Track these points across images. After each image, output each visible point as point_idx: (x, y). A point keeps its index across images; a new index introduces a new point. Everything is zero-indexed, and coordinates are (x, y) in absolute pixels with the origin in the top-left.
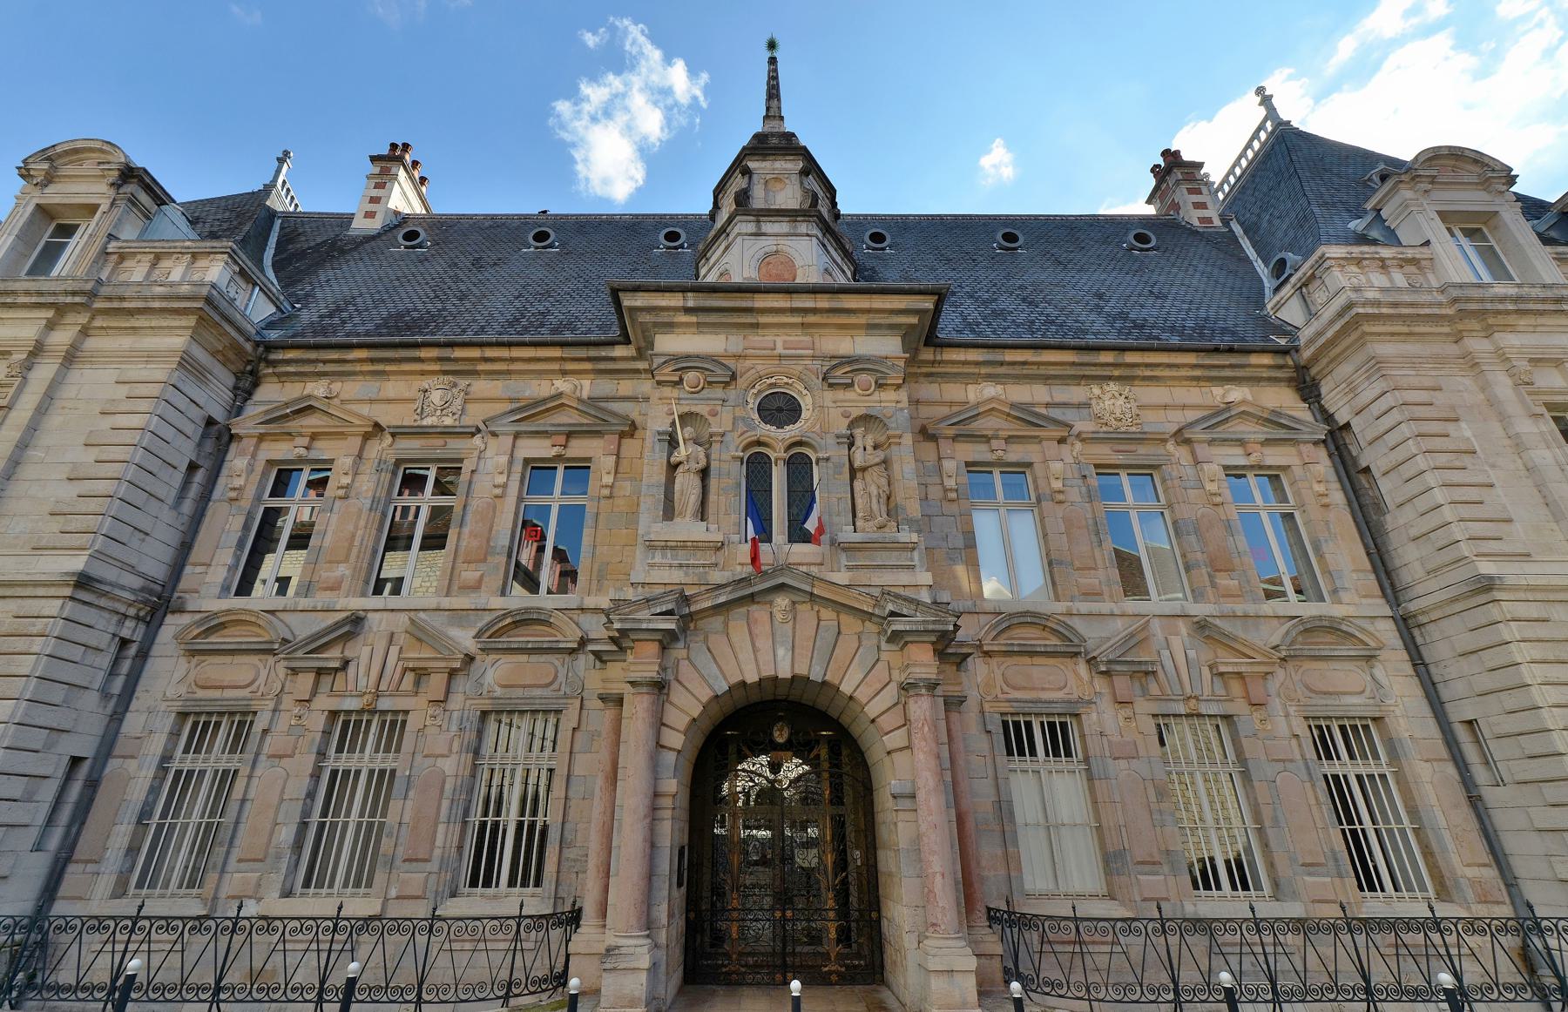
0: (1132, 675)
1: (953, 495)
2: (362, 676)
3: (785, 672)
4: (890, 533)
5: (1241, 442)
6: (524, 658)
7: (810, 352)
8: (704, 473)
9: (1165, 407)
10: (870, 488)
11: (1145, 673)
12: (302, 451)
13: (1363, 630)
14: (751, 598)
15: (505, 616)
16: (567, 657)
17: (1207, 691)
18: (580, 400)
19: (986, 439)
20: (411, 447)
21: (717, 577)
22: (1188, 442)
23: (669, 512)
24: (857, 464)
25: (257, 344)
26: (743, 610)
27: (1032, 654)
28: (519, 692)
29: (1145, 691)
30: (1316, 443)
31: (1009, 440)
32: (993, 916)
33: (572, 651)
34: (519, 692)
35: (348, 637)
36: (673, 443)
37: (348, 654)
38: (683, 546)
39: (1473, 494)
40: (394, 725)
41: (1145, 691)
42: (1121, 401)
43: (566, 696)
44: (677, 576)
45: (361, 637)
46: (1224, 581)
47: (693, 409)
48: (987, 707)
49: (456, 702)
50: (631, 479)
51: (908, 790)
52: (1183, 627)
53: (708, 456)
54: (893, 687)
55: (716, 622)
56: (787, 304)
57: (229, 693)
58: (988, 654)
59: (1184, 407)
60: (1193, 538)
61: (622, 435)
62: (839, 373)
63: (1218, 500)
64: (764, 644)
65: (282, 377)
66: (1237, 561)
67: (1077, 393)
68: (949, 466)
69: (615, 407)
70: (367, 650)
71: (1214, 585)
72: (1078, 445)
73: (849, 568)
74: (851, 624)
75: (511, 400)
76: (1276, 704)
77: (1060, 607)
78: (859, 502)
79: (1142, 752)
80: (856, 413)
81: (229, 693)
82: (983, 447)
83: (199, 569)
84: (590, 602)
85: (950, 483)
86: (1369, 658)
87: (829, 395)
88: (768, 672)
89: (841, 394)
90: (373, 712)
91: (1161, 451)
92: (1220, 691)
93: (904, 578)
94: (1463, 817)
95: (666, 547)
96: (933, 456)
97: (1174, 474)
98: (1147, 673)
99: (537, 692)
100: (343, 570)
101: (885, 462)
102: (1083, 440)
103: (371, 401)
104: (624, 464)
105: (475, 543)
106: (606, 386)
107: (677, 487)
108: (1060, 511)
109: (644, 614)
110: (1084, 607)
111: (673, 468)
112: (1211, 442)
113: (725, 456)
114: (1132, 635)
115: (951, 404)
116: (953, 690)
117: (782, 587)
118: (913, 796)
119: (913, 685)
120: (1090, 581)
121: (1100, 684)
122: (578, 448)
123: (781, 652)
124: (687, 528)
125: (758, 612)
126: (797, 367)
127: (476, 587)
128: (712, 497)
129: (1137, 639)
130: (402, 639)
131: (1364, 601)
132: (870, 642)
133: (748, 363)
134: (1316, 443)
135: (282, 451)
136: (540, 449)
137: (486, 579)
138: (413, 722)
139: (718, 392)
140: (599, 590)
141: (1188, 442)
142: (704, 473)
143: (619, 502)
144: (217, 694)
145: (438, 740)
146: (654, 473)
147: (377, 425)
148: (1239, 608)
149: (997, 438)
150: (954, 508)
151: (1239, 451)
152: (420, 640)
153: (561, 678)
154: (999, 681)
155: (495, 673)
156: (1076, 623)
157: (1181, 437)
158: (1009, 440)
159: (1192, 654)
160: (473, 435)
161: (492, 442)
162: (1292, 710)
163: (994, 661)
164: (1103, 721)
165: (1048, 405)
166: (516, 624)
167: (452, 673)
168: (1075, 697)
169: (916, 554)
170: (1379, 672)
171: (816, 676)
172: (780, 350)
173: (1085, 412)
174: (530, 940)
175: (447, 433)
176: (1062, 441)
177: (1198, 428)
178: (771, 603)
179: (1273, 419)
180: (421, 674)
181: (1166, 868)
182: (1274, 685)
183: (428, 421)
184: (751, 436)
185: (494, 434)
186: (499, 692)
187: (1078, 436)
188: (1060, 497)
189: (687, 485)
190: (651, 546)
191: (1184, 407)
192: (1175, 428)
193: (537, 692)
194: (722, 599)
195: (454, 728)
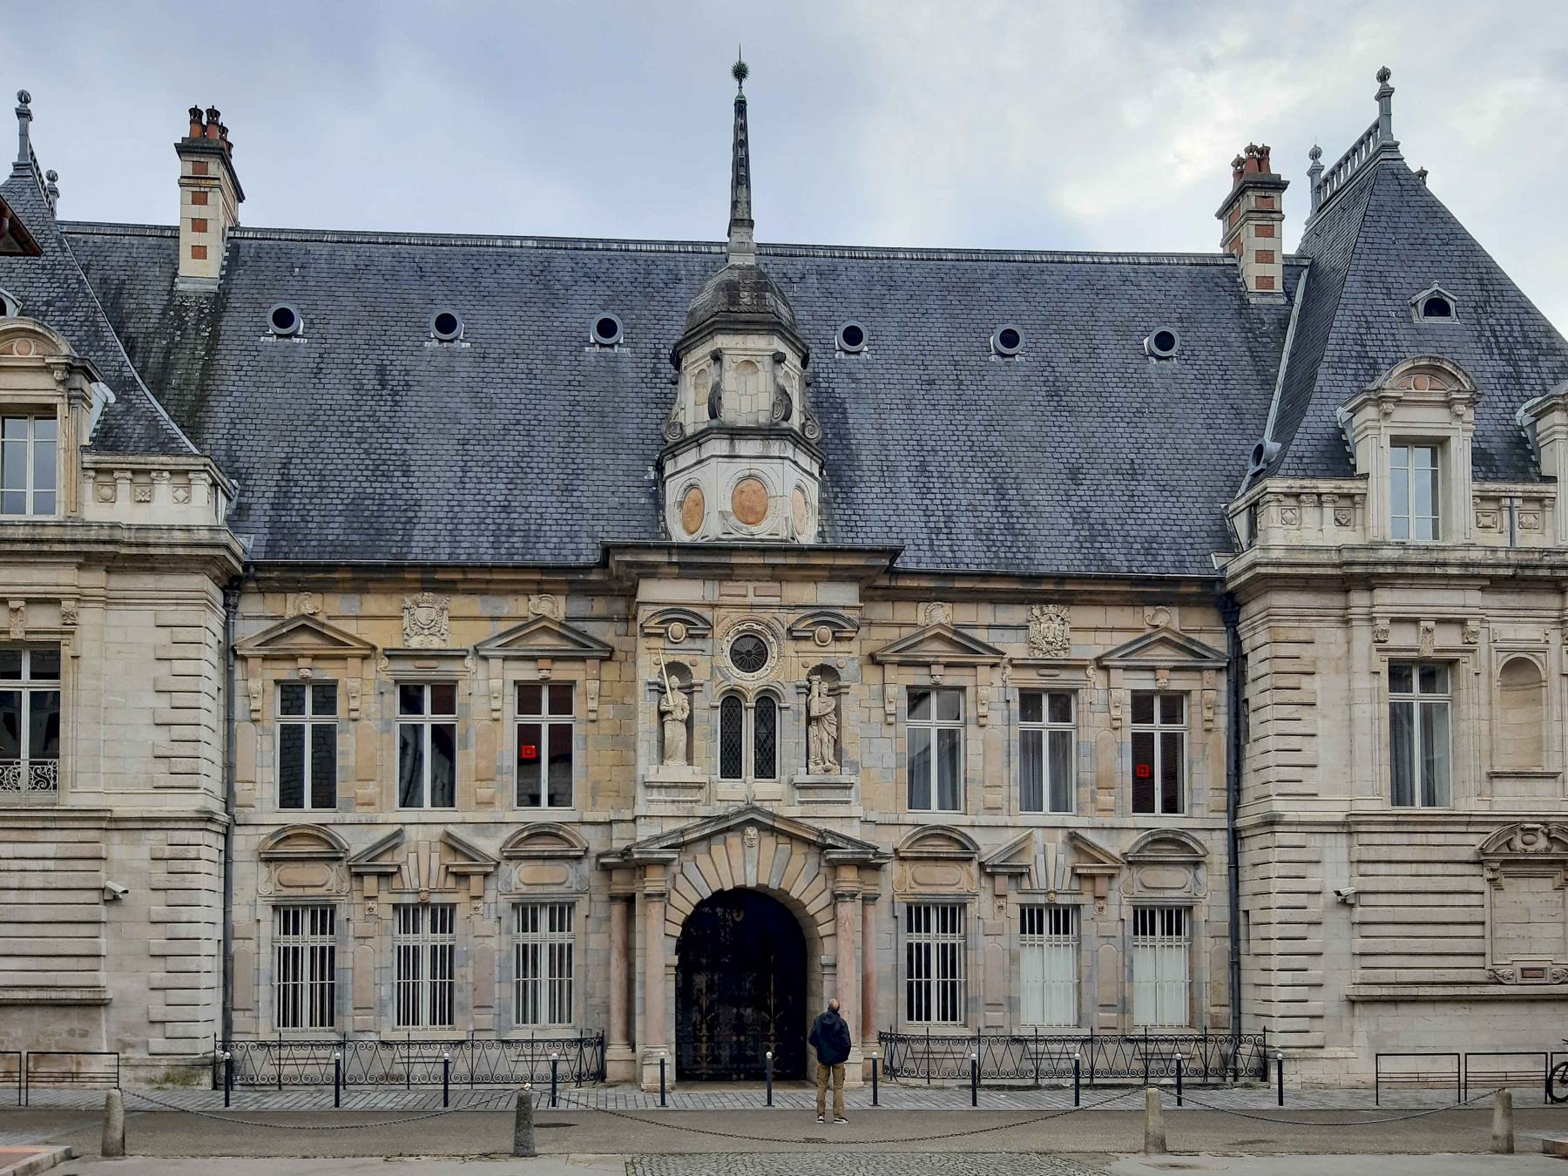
0: (1011, 876)
1: (891, 719)
2: (409, 878)
3: (752, 884)
4: (833, 777)
5: (1153, 669)
6: (540, 862)
7: (775, 601)
8: (689, 723)
9: (1096, 629)
10: (822, 734)
11: (1017, 875)
12: (308, 673)
13: (1195, 840)
14: (728, 829)
15: (523, 830)
16: (575, 863)
17: (1066, 887)
18: (561, 624)
19: (928, 665)
20: (408, 671)
21: (702, 810)
22: (1106, 669)
23: (663, 753)
24: (813, 714)
25: (246, 566)
26: (721, 837)
27: (937, 859)
28: (539, 890)
29: (1018, 886)
30: (1219, 670)
31: (948, 665)
32: (882, 1038)
33: (578, 858)
34: (539, 890)
35: (395, 847)
36: (661, 690)
37: (398, 860)
38: (675, 786)
39: (1294, 742)
40: (443, 917)
41: (1018, 886)
42: (1055, 625)
43: (578, 892)
44: (671, 810)
45: (404, 846)
46: (1105, 799)
47: (677, 659)
48: (897, 899)
49: (490, 895)
50: (614, 702)
51: (831, 961)
52: (1061, 835)
53: (690, 703)
54: (827, 896)
55: (703, 846)
56: (760, 561)
57: (309, 891)
58: (903, 859)
59: (1113, 630)
60: (1087, 760)
61: (603, 660)
62: (800, 627)
63: (1117, 724)
64: (737, 861)
65: (262, 591)
66: (1118, 780)
67: (1016, 615)
68: (891, 691)
69: (592, 629)
70: (412, 856)
71: (1094, 801)
72: (1009, 670)
73: (801, 803)
74: (799, 851)
75: (493, 619)
76: (1114, 897)
77: (966, 820)
78: (812, 746)
79: (1006, 931)
80: (815, 662)
81: (309, 891)
82: (925, 671)
83: (247, 786)
84: (588, 817)
85: (890, 708)
86: (1197, 864)
87: (790, 647)
88: (740, 882)
89: (803, 646)
90: (425, 905)
91: (1080, 675)
92: (1075, 886)
93: (841, 810)
94: (1223, 975)
95: (661, 786)
96: (879, 679)
97: (1087, 699)
98: (1022, 874)
99: (554, 889)
100: (371, 789)
101: (837, 711)
102: (1014, 666)
103: (357, 617)
104: (605, 685)
105: (483, 764)
106: (580, 606)
107: (668, 733)
108: (981, 733)
109: (655, 847)
110: (985, 819)
111: (662, 714)
112: (1126, 669)
113: (706, 705)
114: (1015, 845)
115: (901, 625)
116: (870, 889)
117: (752, 822)
118: (835, 966)
119: (842, 895)
120: (995, 798)
121: (985, 882)
122: (561, 673)
123: (749, 868)
124: (676, 770)
125: (734, 840)
126: (766, 616)
127: (490, 803)
128: (696, 743)
129: (1018, 849)
130: (438, 847)
131: (1212, 815)
132: (813, 860)
133: (723, 611)
134: (1219, 670)
135: (286, 672)
136: (528, 673)
137: (498, 795)
138: (460, 913)
139: (699, 644)
140: (594, 805)
141: (1106, 669)
142: (689, 723)
143: (604, 725)
144: (300, 892)
145: (486, 925)
146: (646, 721)
147: (374, 648)
148: (1108, 821)
149: (937, 663)
150: (891, 731)
151: (1149, 675)
152: (455, 850)
153: (571, 878)
154: (909, 879)
155: (519, 876)
156: (977, 836)
157: (1101, 665)
158: (948, 665)
159: (1061, 858)
160: (463, 657)
161: (482, 664)
162: (1125, 901)
163: (907, 865)
164: (982, 909)
165: (989, 627)
166: (530, 836)
167: (486, 875)
168: (963, 891)
169: (853, 791)
170: (1201, 873)
171: (774, 885)
172: (751, 599)
173: (1022, 633)
174: (588, 1051)
175: (440, 656)
176: (994, 666)
177: (1115, 657)
178: (743, 832)
179: (1185, 646)
180: (462, 877)
181: (1006, 1008)
182: (1116, 884)
183: (415, 643)
184: (725, 686)
185: (485, 658)
186: (524, 889)
187: (1011, 660)
188: (982, 721)
189: (676, 732)
190: (649, 786)
191: (1113, 630)
192: (1099, 652)
193: (554, 889)
194: (708, 831)
195: (493, 916)
